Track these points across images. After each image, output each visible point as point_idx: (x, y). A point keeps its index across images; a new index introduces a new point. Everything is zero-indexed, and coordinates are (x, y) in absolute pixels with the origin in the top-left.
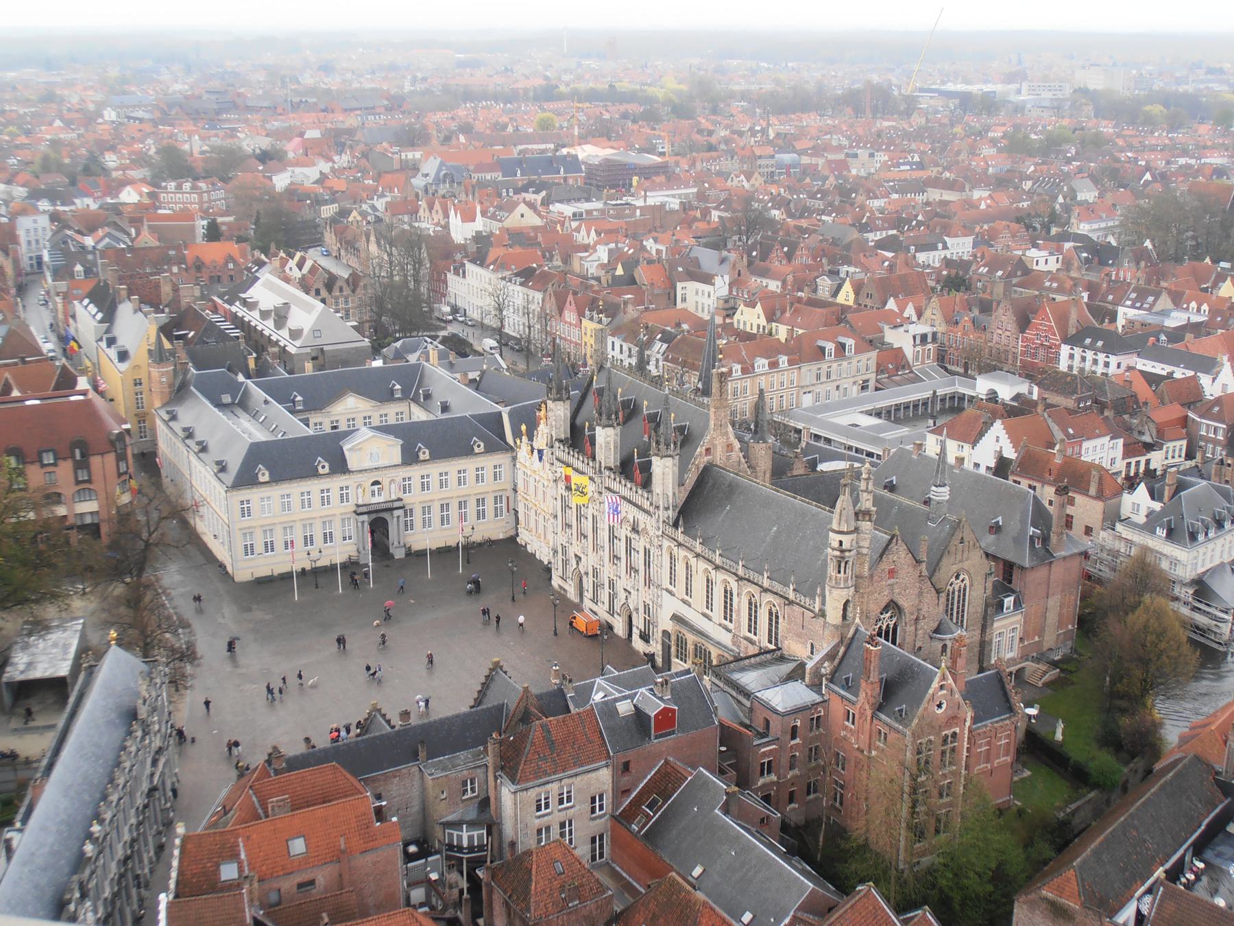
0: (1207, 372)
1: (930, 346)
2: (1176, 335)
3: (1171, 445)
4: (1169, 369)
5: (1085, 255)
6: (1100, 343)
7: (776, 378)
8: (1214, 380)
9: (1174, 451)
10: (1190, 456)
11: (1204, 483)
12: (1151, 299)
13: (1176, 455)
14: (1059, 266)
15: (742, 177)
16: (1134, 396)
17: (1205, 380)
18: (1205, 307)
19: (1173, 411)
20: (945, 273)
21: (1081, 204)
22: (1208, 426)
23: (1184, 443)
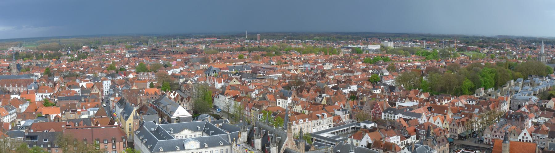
0: (420, 117)
1: (347, 115)
4: (410, 117)
5: (386, 89)
6: (392, 112)
7: (306, 125)
9: (413, 138)
10: (417, 139)
11: (422, 145)
13: (414, 139)
14: (380, 92)
15: (295, 71)
20: (350, 95)
21: (385, 76)
22: (421, 131)
23: (416, 136)
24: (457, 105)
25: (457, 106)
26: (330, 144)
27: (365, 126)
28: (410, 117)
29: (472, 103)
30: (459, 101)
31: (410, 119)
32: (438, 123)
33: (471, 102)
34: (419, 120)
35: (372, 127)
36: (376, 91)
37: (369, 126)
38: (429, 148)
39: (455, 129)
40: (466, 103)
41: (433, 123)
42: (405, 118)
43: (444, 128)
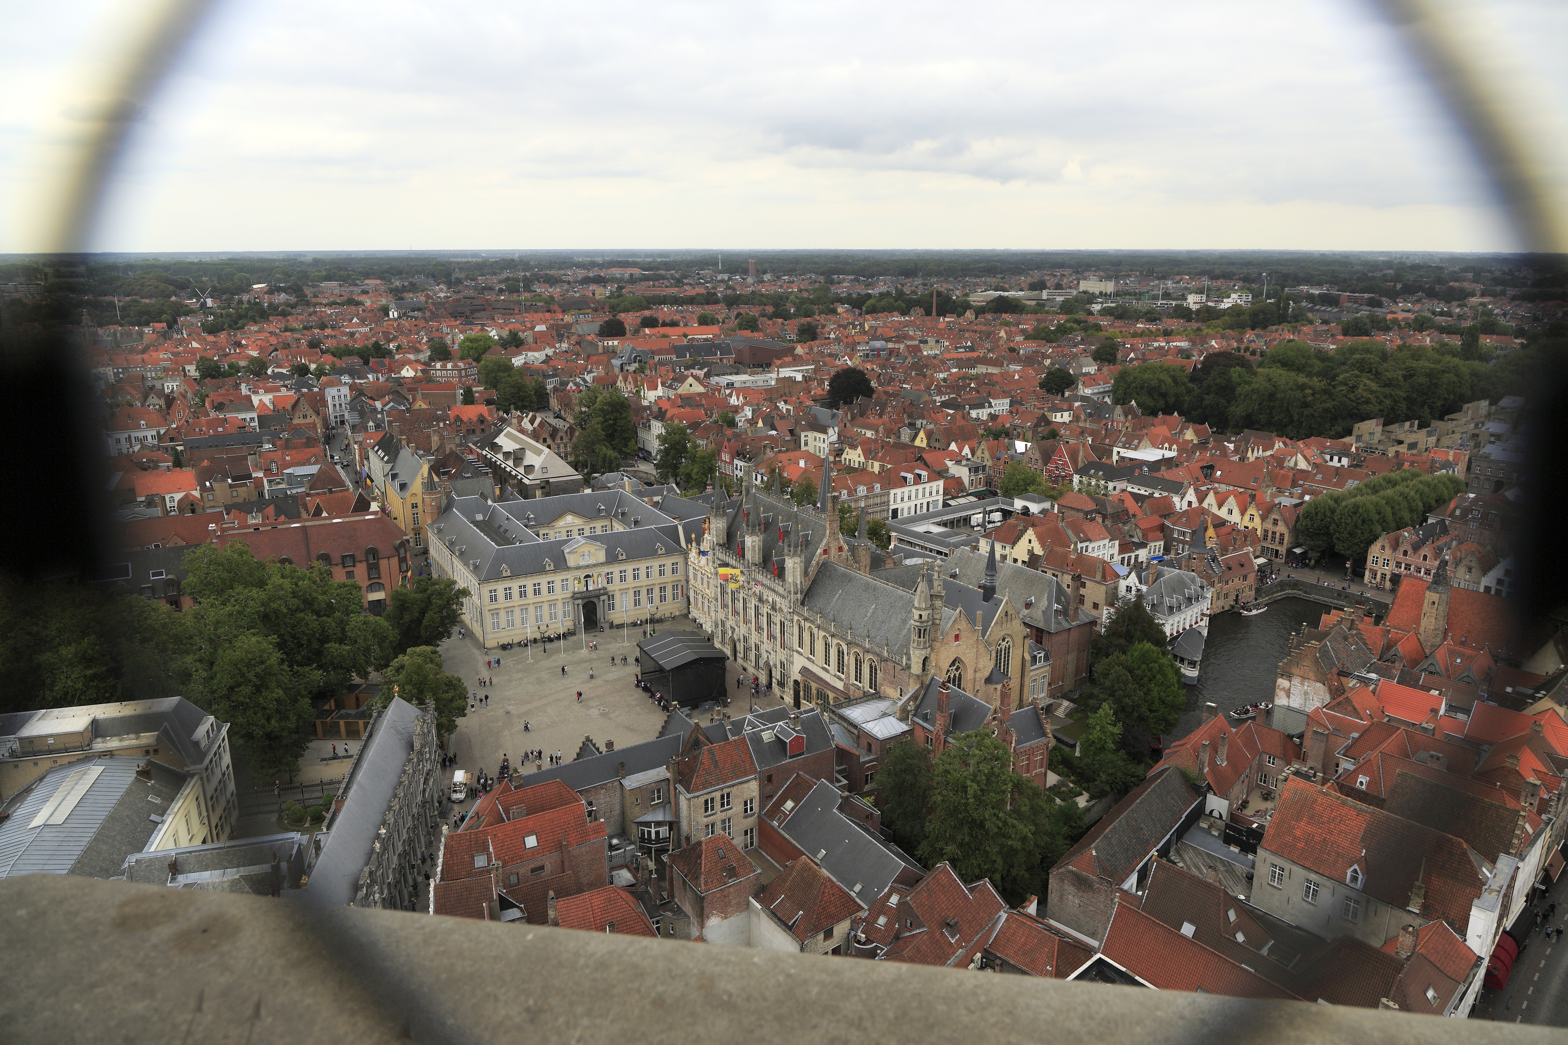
0: (1176, 493)
2: (1155, 466)
3: (1152, 544)
4: (1150, 491)
6: (1101, 473)
8: (1182, 499)
12: (1136, 442)
16: (1126, 511)
17: (1176, 499)
18: (1175, 447)
19: (1156, 521)
23: (1162, 543)
24: (1292, 464)
25: (1292, 469)
29: (1340, 461)
30: (1299, 455)
32: (1230, 512)
34: (1176, 499)
36: (1059, 415)
39: (1278, 535)
40: (1319, 461)
41: (1215, 510)
43: (1246, 527)
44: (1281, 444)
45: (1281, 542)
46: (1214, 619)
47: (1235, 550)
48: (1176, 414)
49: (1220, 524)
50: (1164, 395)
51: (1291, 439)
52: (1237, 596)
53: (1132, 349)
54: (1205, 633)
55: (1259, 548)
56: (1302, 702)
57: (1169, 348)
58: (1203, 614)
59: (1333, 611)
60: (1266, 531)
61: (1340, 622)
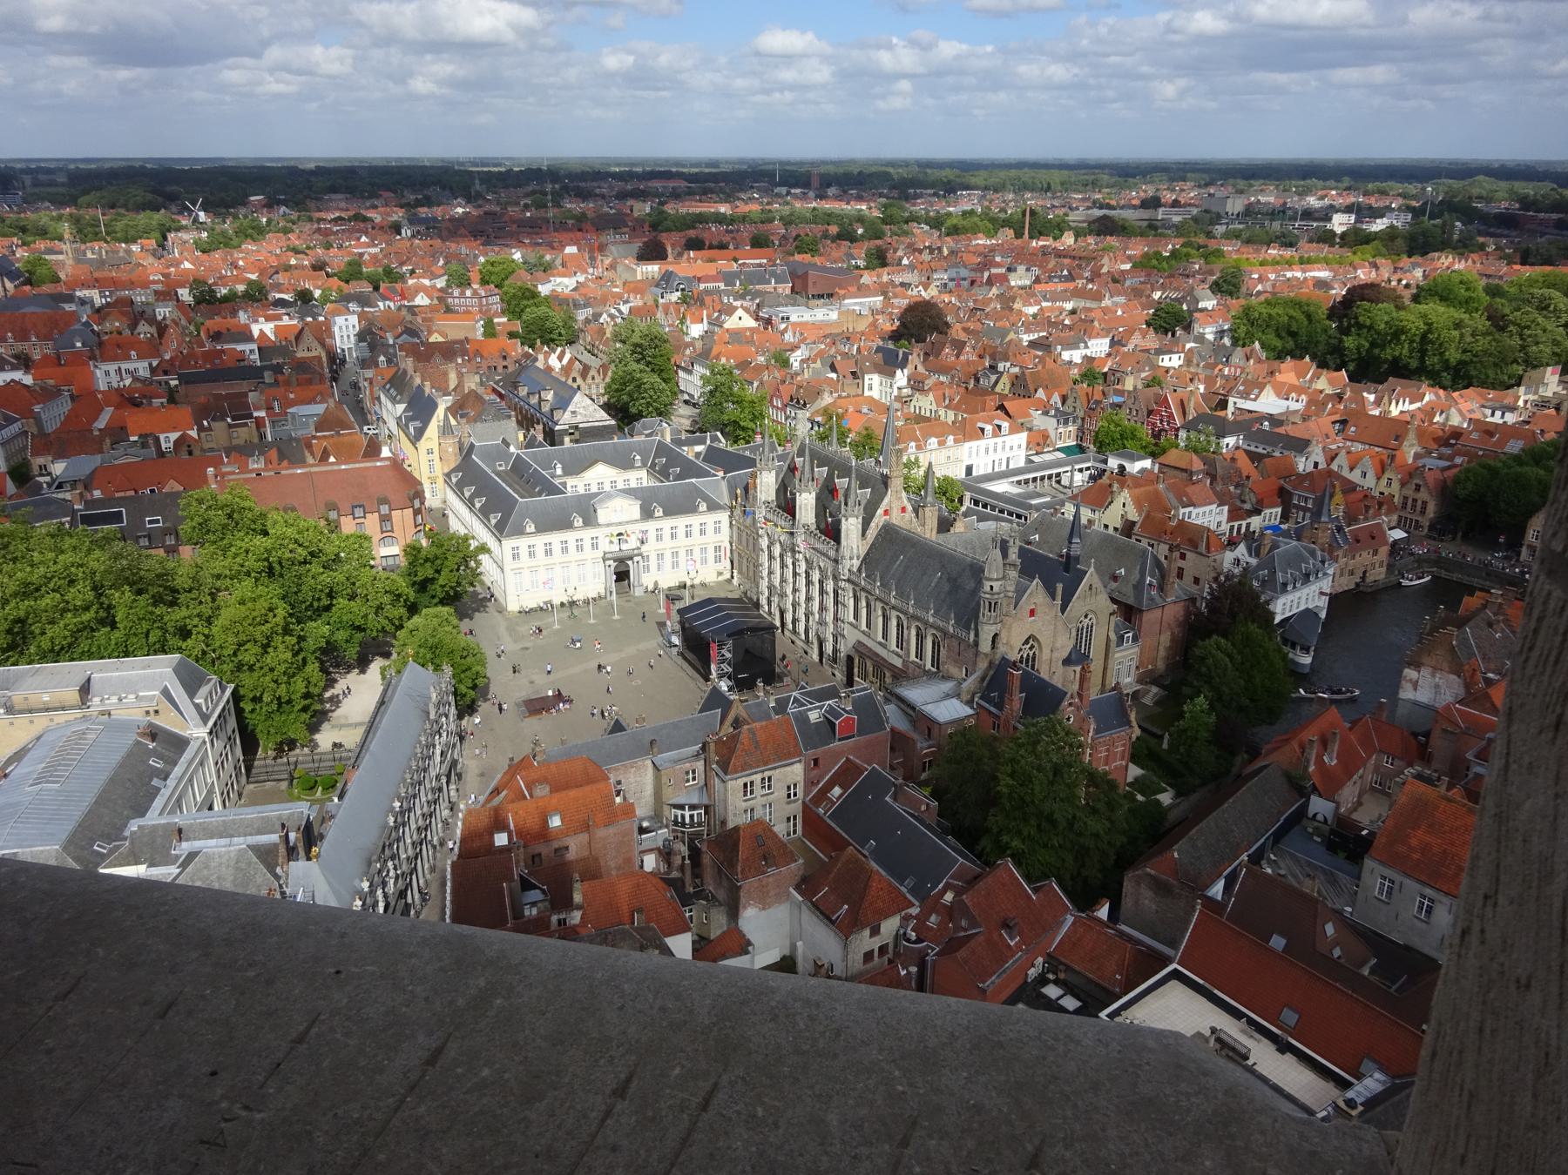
1: (1071, 428)
3: (1268, 511)
4: (1269, 449)
7: (944, 453)
12: (1256, 391)
14: (1181, 362)
21: (1202, 310)
23: (1280, 510)
26: (1010, 514)
27: (1122, 468)
28: (1269, 449)
31: (1268, 455)
32: (1364, 475)
33: (1498, 413)
35: (1143, 470)
36: (1166, 357)
37: (1135, 467)
38: (1319, 553)
39: (1419, 503)
40: (1477, 416)
41: (1346, 473)
42: (1252, 448)
43: (1382, 493)
44: (1433, 398)
45: (1423, 512)
46: (1335, 600)
47: (1366, 519)
48: (1307, 358)
49: (1350, 488)
50: (1293, 334)
51: (1444, 388)
52: (1365, 572)
53: (1260, 280)
54: (1323, 615)
55: (1395, 517)
56: (1432, 696)
57: (1305, 278)
58: (1322, 593)
59: (1478, 593)
60: (1406, 498)
61: (1484, 607)
